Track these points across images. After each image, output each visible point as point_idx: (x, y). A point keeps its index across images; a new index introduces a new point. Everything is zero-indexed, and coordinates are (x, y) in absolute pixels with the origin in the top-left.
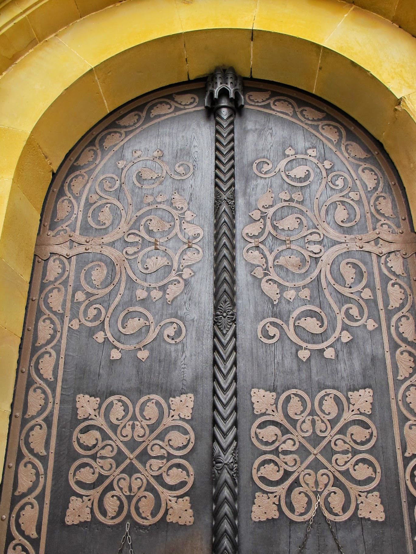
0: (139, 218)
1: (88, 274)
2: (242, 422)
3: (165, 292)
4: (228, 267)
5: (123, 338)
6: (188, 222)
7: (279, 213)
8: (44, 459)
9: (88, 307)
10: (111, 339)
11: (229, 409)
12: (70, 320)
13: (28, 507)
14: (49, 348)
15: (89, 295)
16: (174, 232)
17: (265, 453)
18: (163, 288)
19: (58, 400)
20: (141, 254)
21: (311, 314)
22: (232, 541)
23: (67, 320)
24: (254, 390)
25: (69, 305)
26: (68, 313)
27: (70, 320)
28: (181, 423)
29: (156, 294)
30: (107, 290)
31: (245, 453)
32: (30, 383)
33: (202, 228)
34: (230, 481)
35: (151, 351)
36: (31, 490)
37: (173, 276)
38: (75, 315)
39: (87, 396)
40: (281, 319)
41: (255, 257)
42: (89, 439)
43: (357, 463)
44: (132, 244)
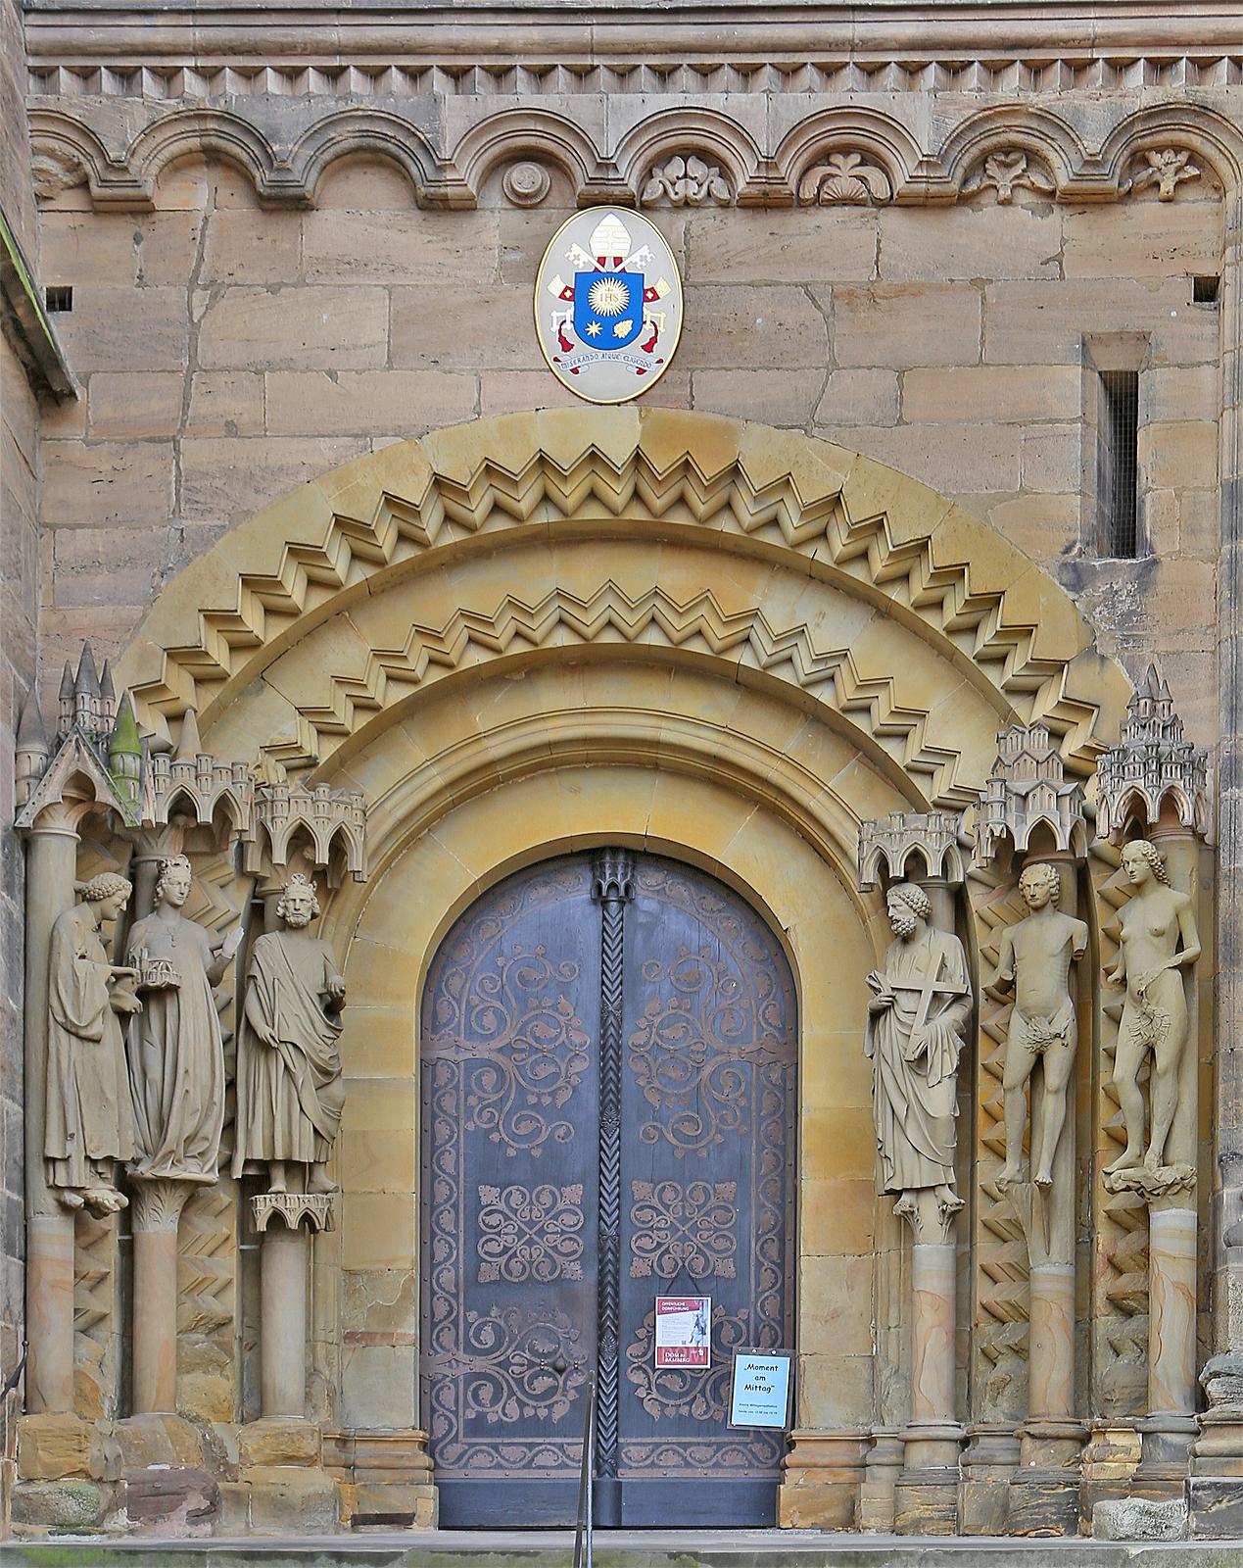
0: (525, 1024)
1: (479, 1079)
2: (624, 1209)
3: (554, 1099)
4: (614, 1078)
5: (517, 1138)
6: (575, 1029)
7: (665, 1022)
8: (456, 1237)
9: (481, 1110)
10: (506, 1139)
11: (613, 1196)
12: (466, 1123)
13: (445, 1272)
14: (448, 1147)
15: (481, 1099)
16: (561, 1039)
17: (643, 1229)
18: (553, 1094)
19: (462, 1189)
20: (530, 1060)
21: (689, 1119)
22: (613, 1300)
23: (462, 1122)
24: (635, 1182)
25: (462, 1108)
26: (462, 1115)
27: (466, 1123)
28: (572, 1207)
29: (546, 1101)
30: (502, 1092)
31: (625, 1228)
32: (434, 1176)
33: (589, 1035)
34: (613, 1248)
35: (544, 1149)
36: (446, 1259)
37: (561, 1083)
38: (469, 1118)
39: (488, 1187)
40: (661, 1123)
41: (639, 1067)
42: (493, 1220)
43: (717, 1237)
44: (523, 1051)
